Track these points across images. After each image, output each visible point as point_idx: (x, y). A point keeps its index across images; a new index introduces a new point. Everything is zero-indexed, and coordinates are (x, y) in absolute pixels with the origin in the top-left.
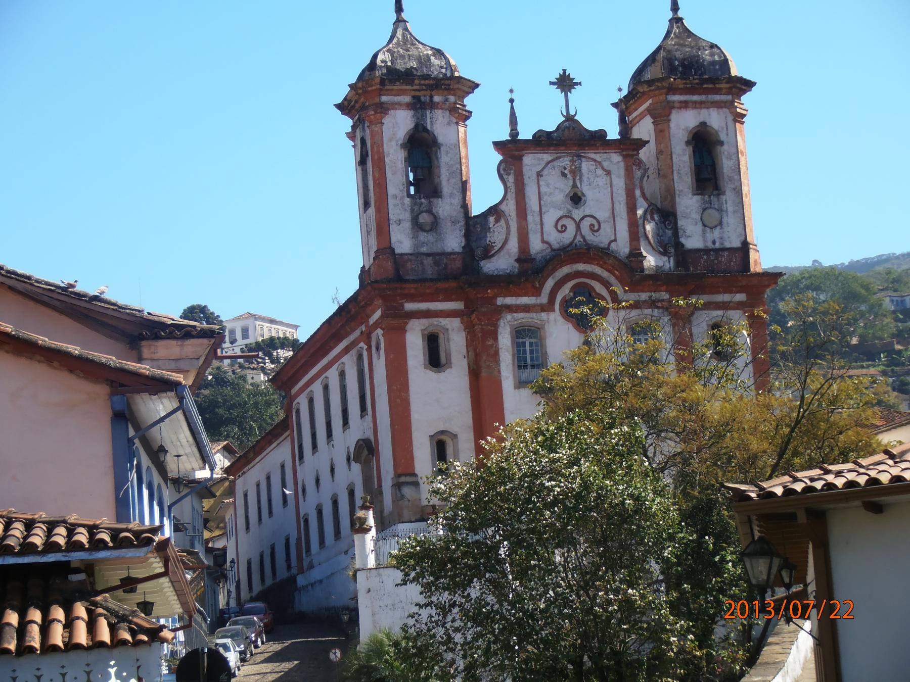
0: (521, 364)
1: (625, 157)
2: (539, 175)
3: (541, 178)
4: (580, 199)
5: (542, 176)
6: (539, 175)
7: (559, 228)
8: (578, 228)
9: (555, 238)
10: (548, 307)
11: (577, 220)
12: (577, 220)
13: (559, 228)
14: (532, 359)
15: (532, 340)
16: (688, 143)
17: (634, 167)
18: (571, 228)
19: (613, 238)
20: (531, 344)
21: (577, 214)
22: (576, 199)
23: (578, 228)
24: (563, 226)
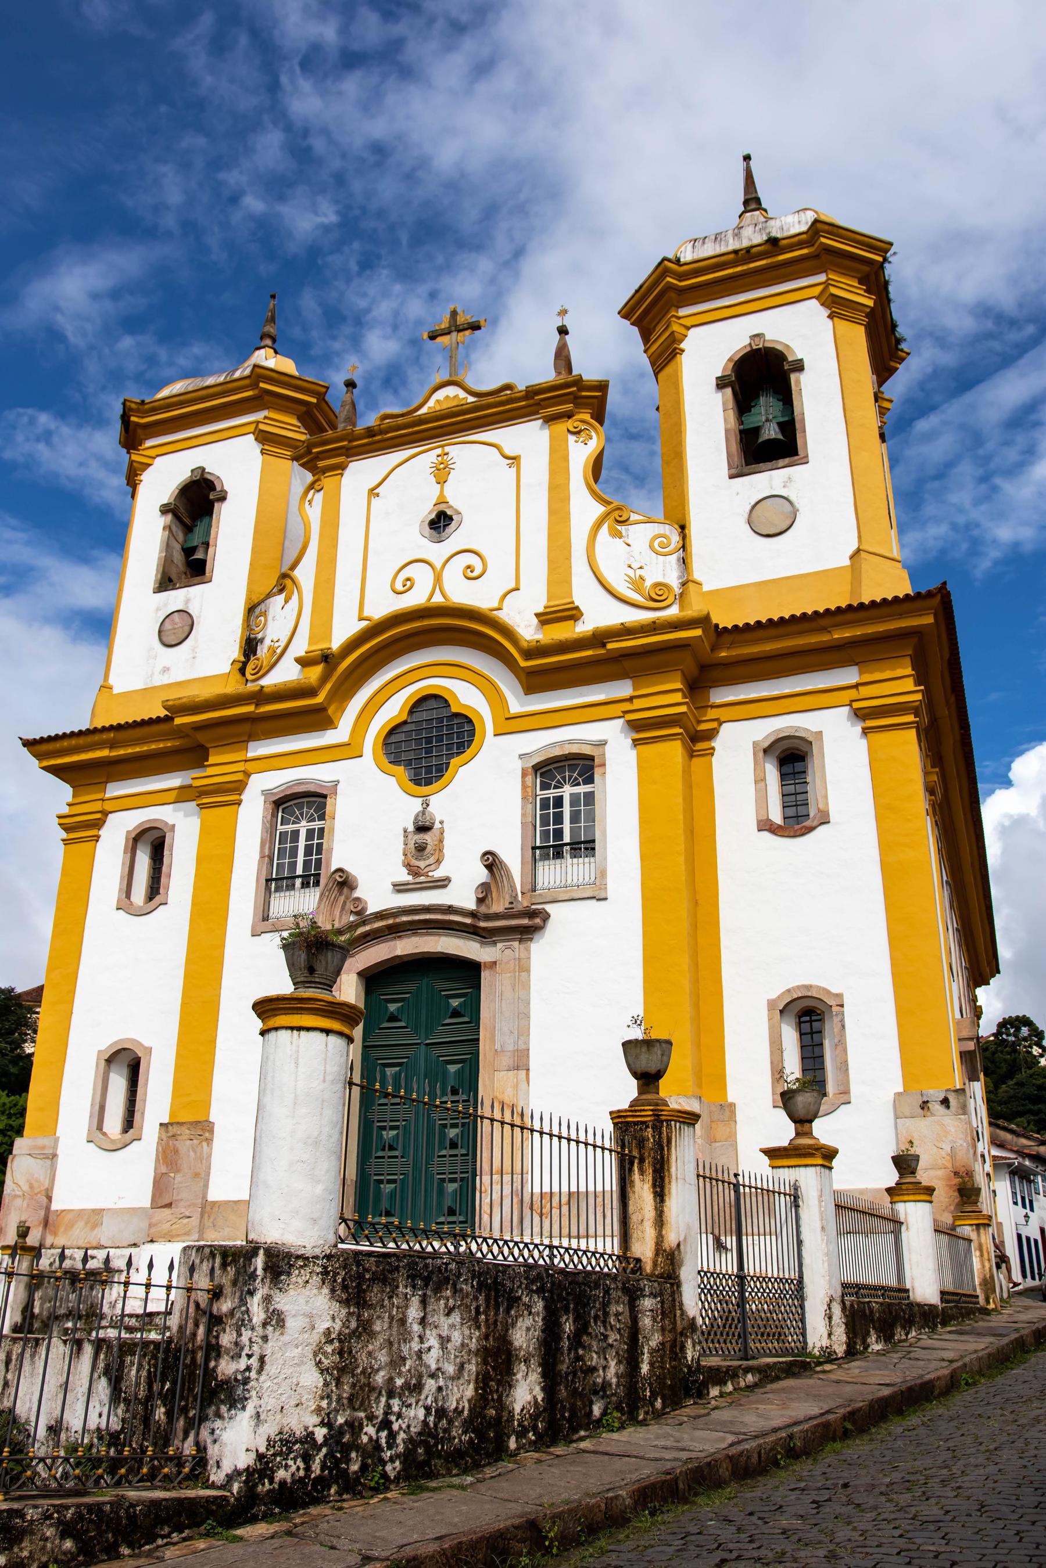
0: (276, 881)
1: (549, 420)
2: (373, 492)
3: (375, 501)
4: (451, 519)
5: (378, 495)
6: (373, 492)
7: (399, 587)
8: (438, 579)
9: (383, 605)
10: (348, 750)
11: (438, 566)
12: (438, 566)
13: (399, 587)
14: (307, 864)
15: (316, 825)
16: (721, 383)
17: (572, 438)
18: (423, 577)
19: (513, 585)
20: (310, 834)
21: (437, 552)
22: (441, 522)
23: (438, 579)
24: (408, 579)
